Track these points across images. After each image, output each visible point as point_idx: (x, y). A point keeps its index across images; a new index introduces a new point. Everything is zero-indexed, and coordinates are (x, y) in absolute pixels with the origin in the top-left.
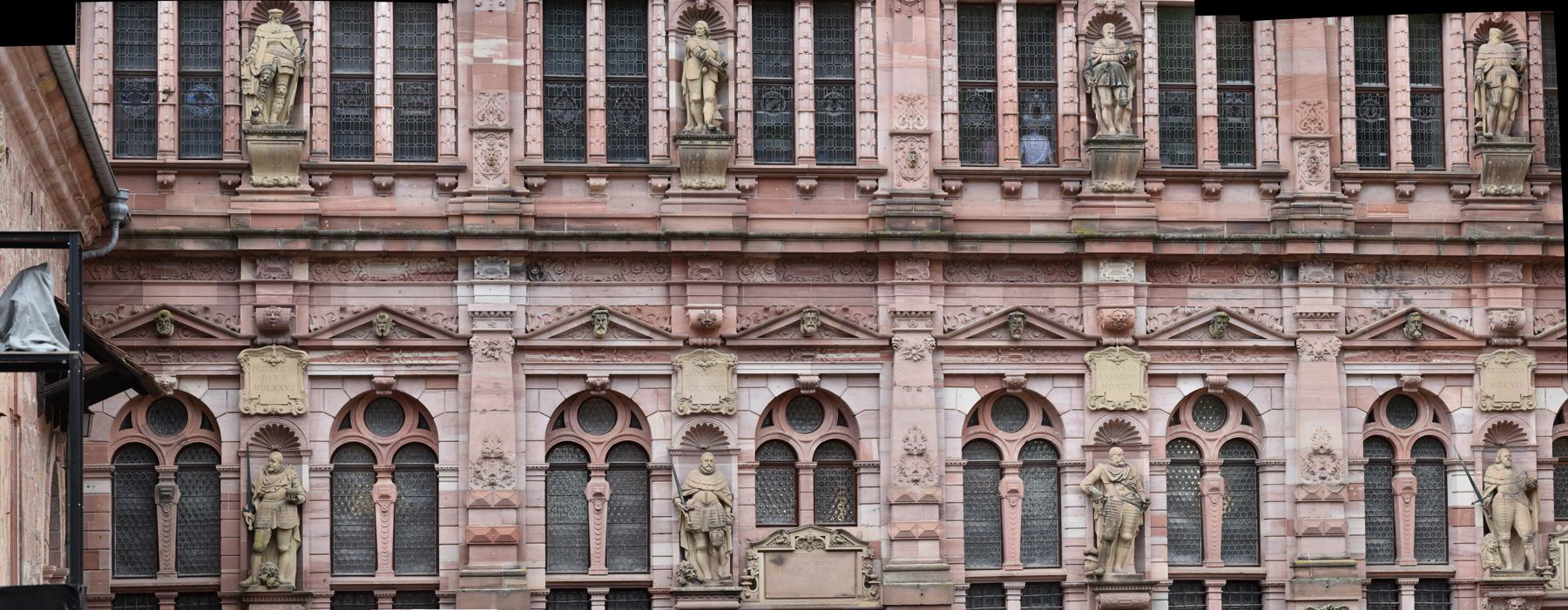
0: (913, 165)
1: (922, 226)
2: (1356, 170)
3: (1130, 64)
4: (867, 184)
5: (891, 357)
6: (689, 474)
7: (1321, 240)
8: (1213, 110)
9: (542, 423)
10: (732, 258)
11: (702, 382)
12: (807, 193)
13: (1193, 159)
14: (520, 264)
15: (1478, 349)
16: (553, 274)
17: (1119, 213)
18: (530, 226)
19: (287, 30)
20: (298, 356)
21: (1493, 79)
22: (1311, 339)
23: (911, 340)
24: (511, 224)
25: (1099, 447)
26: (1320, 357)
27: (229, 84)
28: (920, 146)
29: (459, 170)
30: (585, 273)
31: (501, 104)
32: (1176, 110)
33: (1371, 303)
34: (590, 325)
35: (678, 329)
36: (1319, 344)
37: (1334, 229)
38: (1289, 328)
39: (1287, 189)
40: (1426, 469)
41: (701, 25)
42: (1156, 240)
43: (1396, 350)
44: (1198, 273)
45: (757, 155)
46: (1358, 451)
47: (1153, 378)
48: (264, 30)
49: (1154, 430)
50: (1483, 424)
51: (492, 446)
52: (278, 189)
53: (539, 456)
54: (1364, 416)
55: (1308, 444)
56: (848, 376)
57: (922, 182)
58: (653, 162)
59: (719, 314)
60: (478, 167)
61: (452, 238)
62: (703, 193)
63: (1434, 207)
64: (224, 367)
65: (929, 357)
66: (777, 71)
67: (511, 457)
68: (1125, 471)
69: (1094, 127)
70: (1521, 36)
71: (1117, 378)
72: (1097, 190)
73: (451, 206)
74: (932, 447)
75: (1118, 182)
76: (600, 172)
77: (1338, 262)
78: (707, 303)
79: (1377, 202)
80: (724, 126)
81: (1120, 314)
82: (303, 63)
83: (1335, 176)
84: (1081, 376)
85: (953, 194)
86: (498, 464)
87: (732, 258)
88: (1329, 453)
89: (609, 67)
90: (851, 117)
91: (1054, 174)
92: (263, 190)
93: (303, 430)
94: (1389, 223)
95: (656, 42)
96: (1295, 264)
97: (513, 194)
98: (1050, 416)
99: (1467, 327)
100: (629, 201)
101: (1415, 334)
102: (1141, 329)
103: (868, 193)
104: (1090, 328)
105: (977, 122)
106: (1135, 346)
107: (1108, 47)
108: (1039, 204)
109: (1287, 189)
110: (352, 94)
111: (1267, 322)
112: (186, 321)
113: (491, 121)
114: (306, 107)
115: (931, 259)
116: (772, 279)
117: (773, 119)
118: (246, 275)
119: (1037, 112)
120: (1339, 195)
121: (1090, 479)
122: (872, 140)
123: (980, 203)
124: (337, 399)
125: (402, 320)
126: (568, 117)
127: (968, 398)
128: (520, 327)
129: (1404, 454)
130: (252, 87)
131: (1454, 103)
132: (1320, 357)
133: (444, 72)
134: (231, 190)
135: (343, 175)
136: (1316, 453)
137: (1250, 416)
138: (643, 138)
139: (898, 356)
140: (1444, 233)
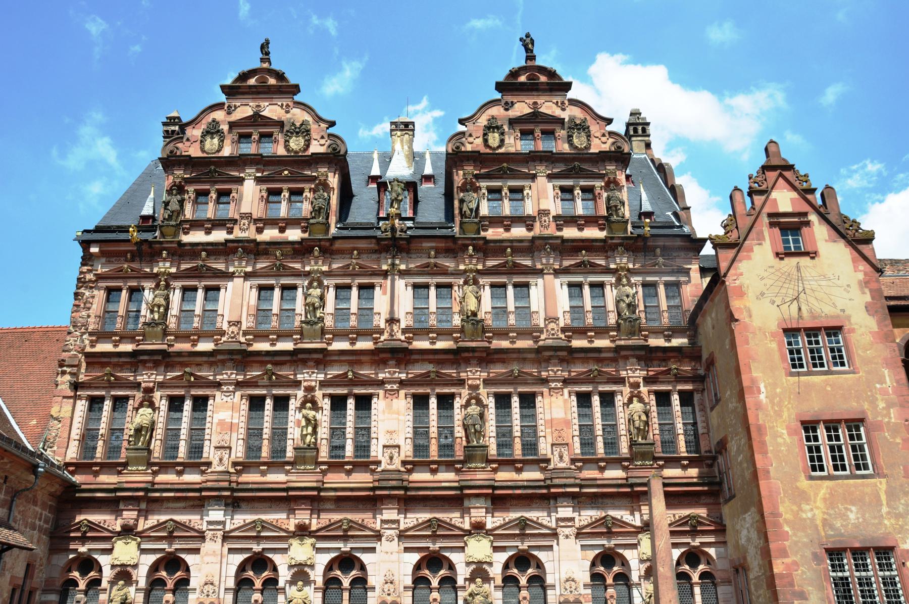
0: (391, 458)
1: (394, 483)
2: (581, 457)
3: (482, 416)
4: (373, 467)
5: (380, 540)
6: (292, 591)
7: (565, 486)
8: (519, 434)
9: (233, 570)
10: (315, 500)
11: (300, 551)
12: (349, 473)
13: (512, 455)
14: (229, 501)
15: (639, 533)
16: (243, 505)
17: (478, 477)
18: (234, 485)
19: (150, 410)
20: (136, 540)
21: (636, 418)
22: (564, 529)
23: (389, 532)
24: (226, 484)
25: (471, 579)
26: (567, 537)
27: (126, 431)
28: (395, 451)
29: (209, 464)
30: (256, 505)
31: (227, 437)
32: (504, 435)
33: (588, 515)
34: (254, 527)
35: (292, 528)
36: (567, 531)
37: (571, 481)
38: (554, 525)
39: (551, 466)
40: (619, 587)
41: (309, 405)
42: (494, 488)
43: (602, 534)
44: (515, 502)
45: (331, 457)
46: (588, 580)
47: (496, 549)
48: (141, 411)
49: (496, 571)
50: (643, 567)
51: (210, 578)
52: (138, 472)
53: (231, 583)
54: (589, 563)
55: (564, 577)
56: (363, 548)
57: (397, 465)
58: (287, 459)
59: (307, 522)
60: (215, 462)
61: (200, 490)
62: (305, 472)
63: (615, 473)
64: (108, 546)
65: (396, 539)
66: (340, 423)
67: (217, 583)
68: (481, 589)
69: (468, 442)
70: (647, 401)
71: (479, 548)
72: (469, 468)
73: (203, 478)
74: (396, 579)
75: (479, 465)
76: (264, 464)
77: (573, 496)
78: (303, 516)
79: (590, 473)
80: (315, 444)
81: (479, 519)
82: (153, 423)
83: (573, 461)
84: (463, 548)
85: (410, 471)
86: (211, 586)
87: (315, 500)
88: (573, 580)
89: (273, 423)
90: (369, 442)
91: (451, 461)
92: (132, 473)
93: (134, 573)
94: (596, 479)
95: (291, 412)
96: (556, 496)
97: (228, 472)
98: (451, 567)
99: (633, 523)
100: (277, 478)
101: (608, 528)
102: (489, 526)
103: (373, 472)
104: (467, 526)
105: (421, 442)
106: (487, 534)
107: (474, 409)
108: (447, 477)
109: (551, 466)
110: (172, 435)
111: (545, 523)
112: (92, 526)
113: (223, 444)
114: (153, 440)
115: (398, 499)
116: (332, 507)
117: (337, 442)
118: (122, 507)
119: (446, 437)
120: (573, 467)
121: (467, 593)
122: (376, 451)
123: (421, 476)
124: (151, 559)
125: (179, 525)
126: (257, 443)
127: (415, 557)
128: (228, 528)
129: (610, 581)
130: (132, 432)
131: (622, 428)
132: (567, 537)
133: (208, 425)
134: (119, 473)
135: (164, 467)
136: (567, 580)
137: (540, 565)
138: (284, 451)
139: (383, 539)
140: (620, 482)
